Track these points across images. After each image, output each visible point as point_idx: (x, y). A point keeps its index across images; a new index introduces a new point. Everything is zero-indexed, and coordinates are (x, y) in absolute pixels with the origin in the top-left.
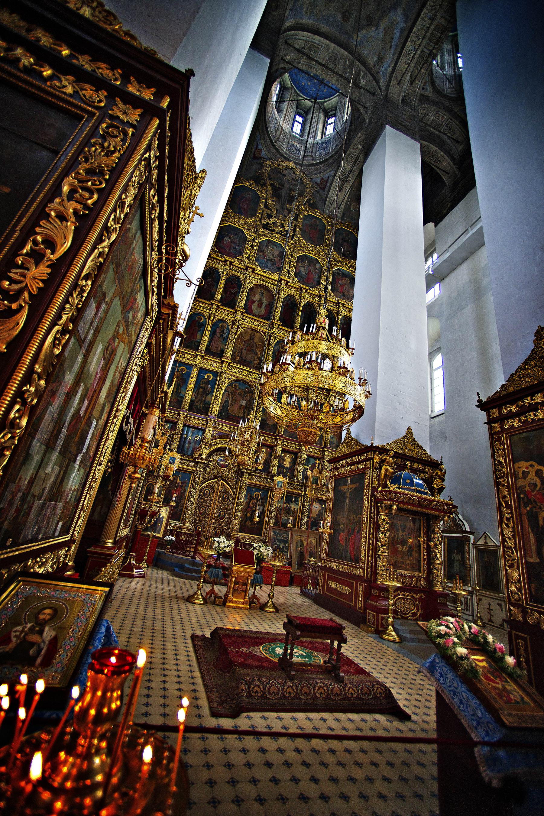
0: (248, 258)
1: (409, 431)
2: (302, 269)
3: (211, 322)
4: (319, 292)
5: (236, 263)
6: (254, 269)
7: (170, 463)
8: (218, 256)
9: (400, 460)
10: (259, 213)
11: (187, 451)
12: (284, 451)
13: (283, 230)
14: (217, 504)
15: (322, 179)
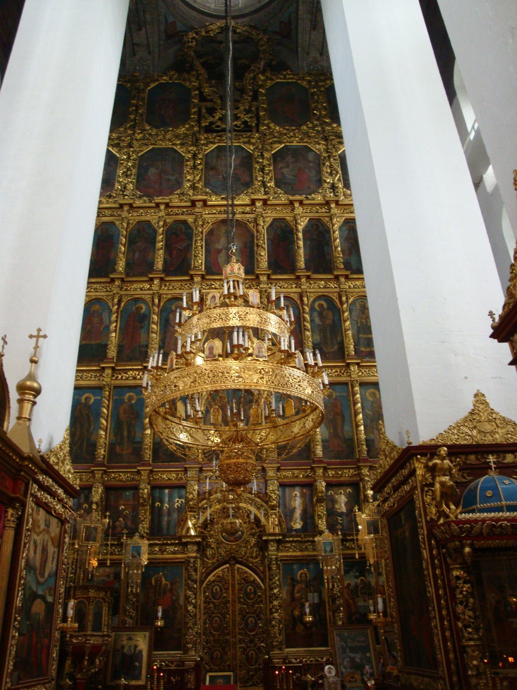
0: (194, 187)
1: (477, 398)
2: (285, 171)
3: (156, 309)
4: (324, 196)
5: (175, 201)
6: (205, 202)
7: (133, 556)
8: (145, 202)
9: (472, 457)
10: (194, 113)
11: (168, 528)
12: (329, 485)
13: (238, 123)
14: (238, 606)
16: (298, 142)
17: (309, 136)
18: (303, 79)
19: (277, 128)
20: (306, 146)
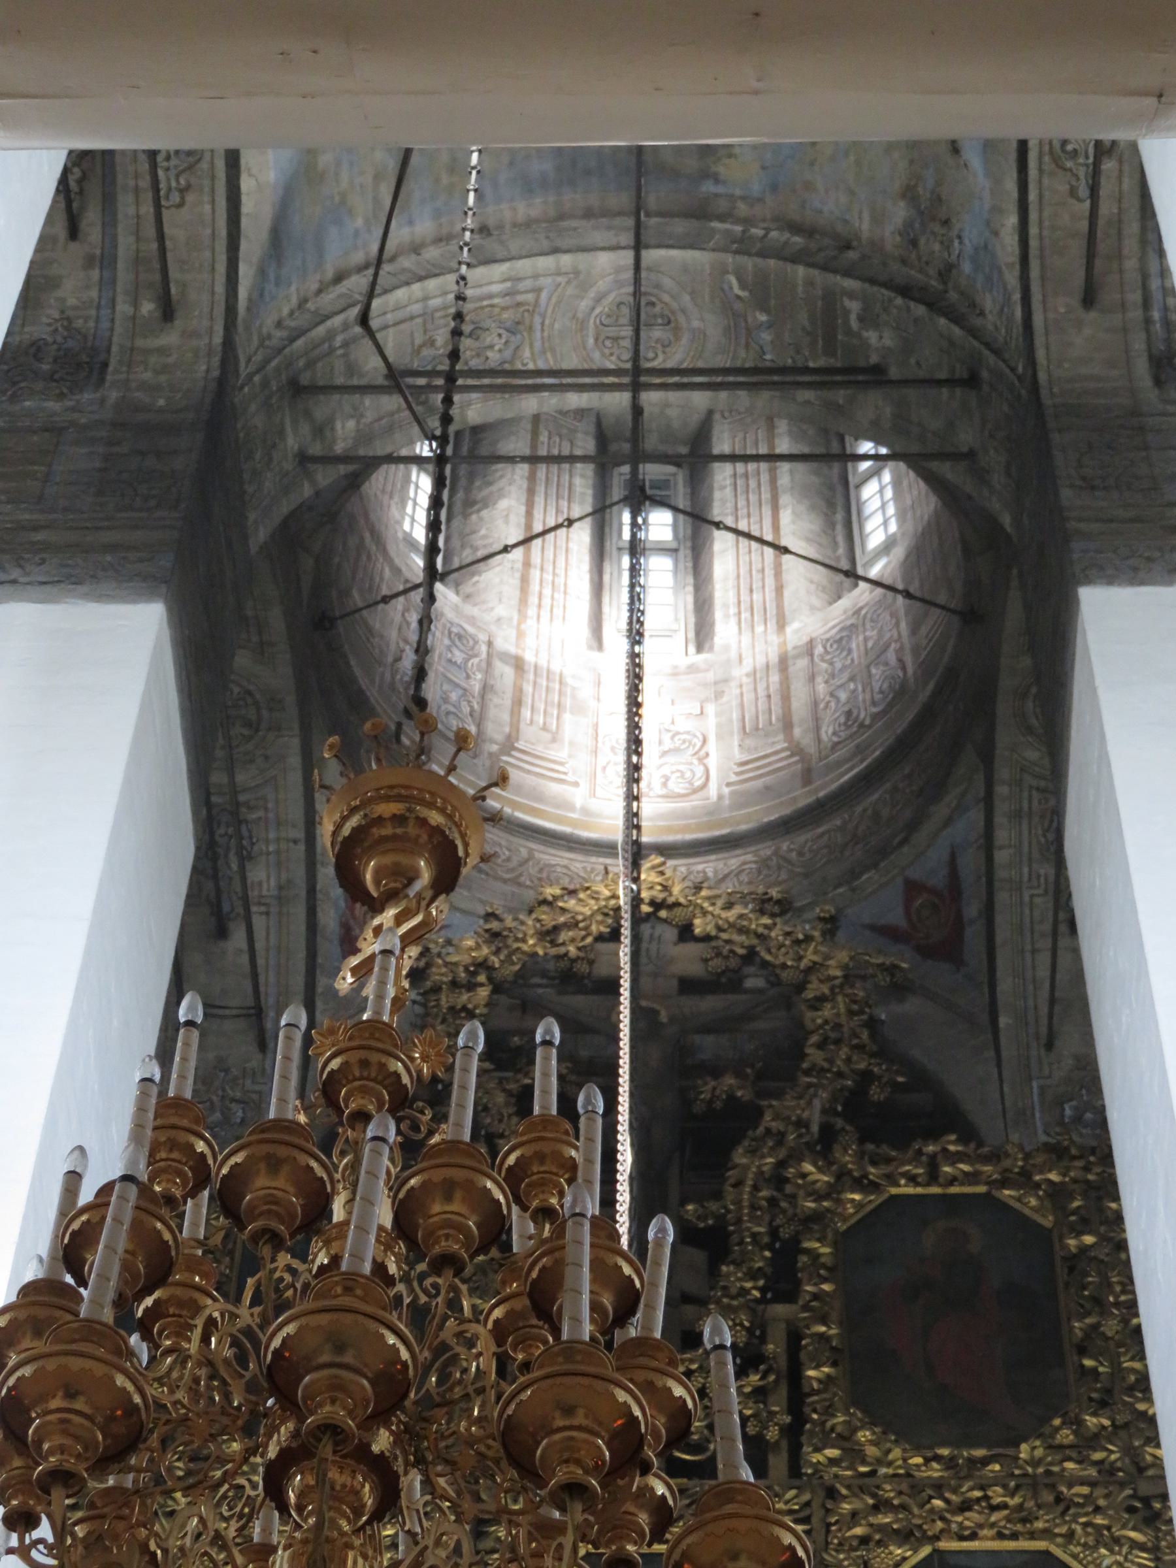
15: (912, 888)
16: (1000, 1536)
17: (1059, 1499)
18: (1024, 1180)
19: (896, 1453)
20: (1047, 1553)
